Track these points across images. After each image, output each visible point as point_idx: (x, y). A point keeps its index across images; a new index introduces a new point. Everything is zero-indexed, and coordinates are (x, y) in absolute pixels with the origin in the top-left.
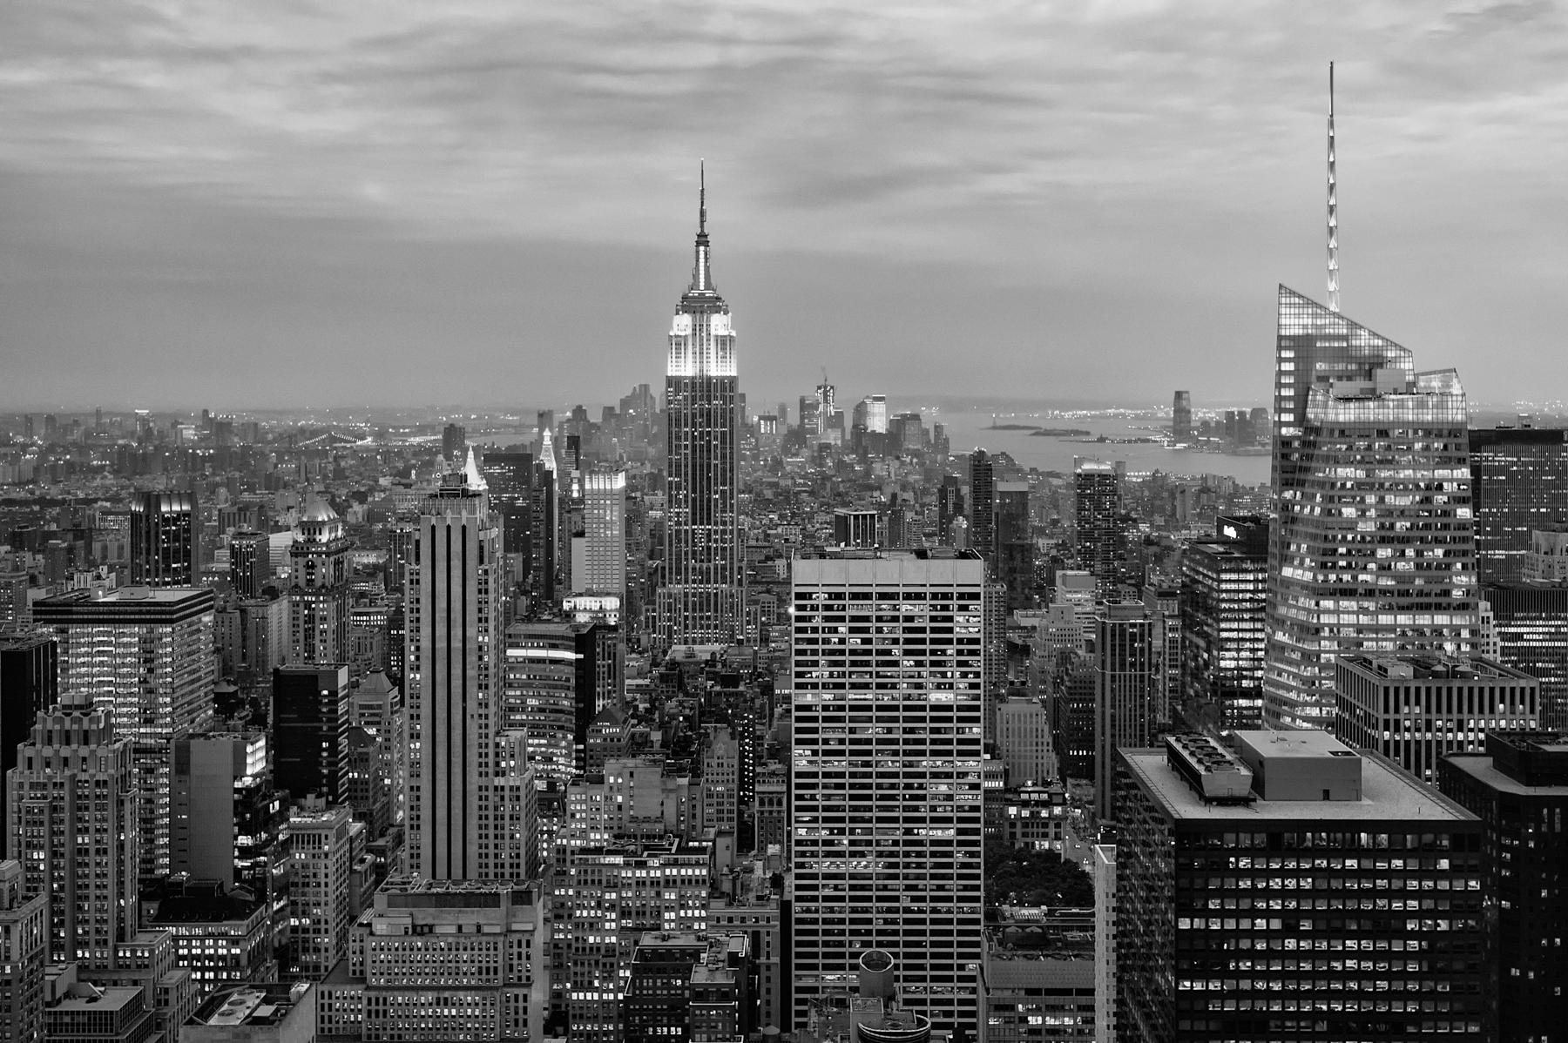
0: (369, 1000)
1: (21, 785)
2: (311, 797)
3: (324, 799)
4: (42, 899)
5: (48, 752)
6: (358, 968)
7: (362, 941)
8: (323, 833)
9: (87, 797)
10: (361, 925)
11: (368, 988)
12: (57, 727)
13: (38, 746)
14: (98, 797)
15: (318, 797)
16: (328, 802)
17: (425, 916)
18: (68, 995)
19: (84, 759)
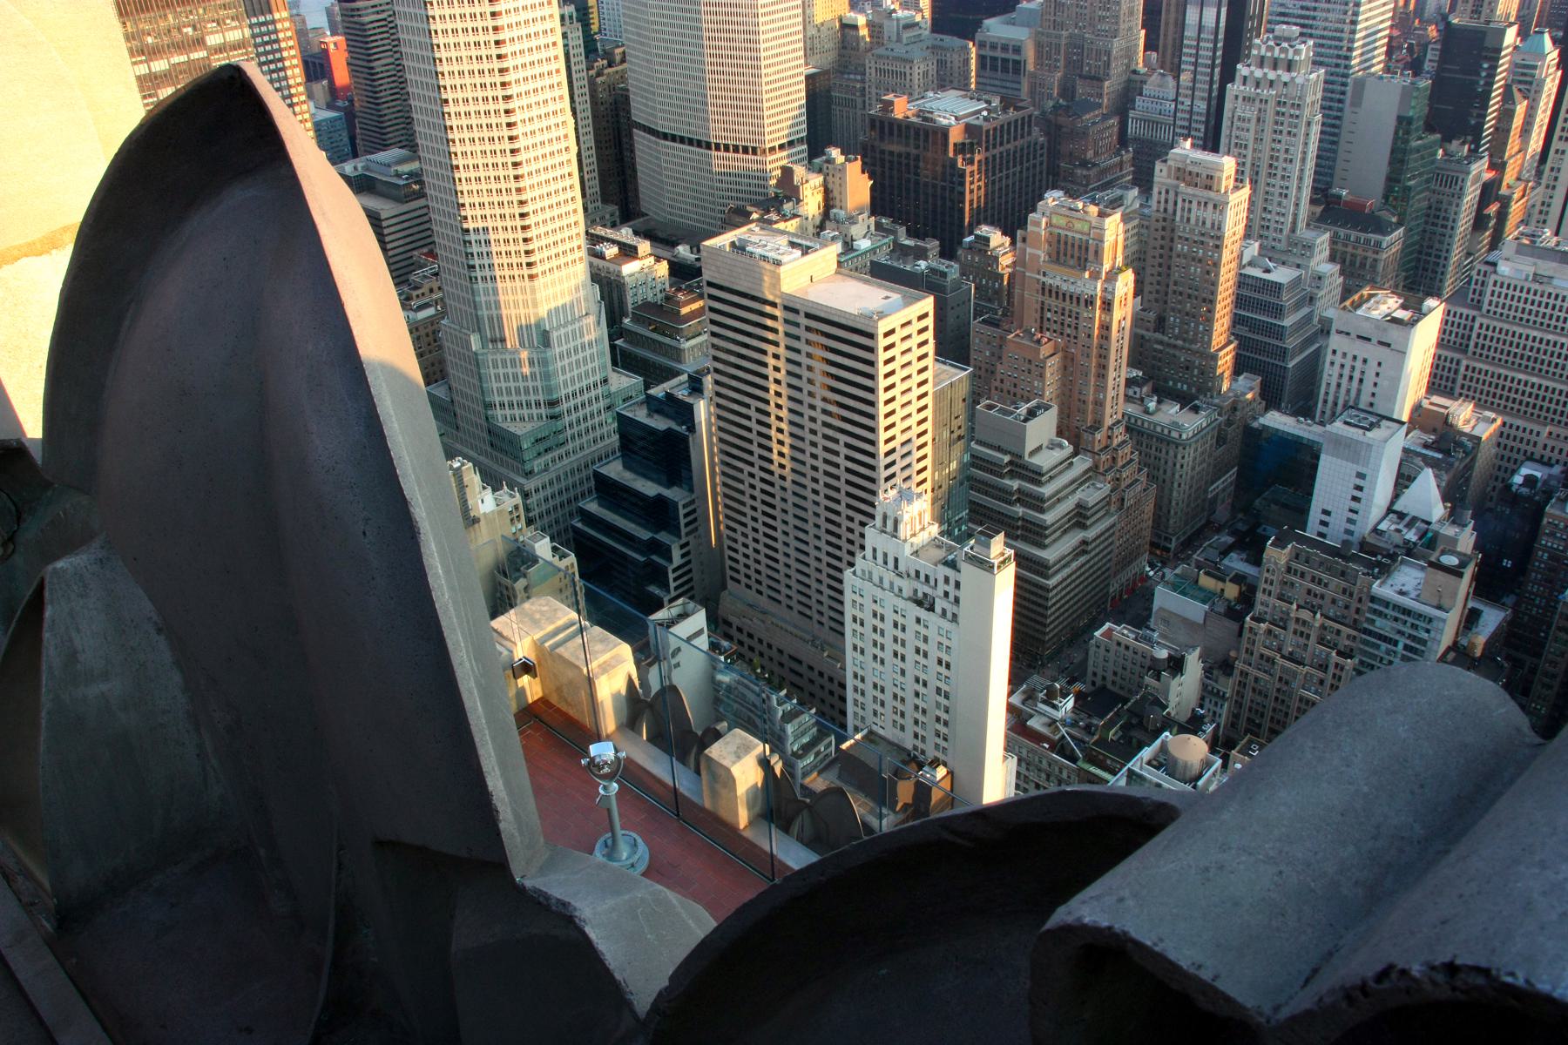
0: (1481, 325)
1: (1237, 97)
2: (1455, 143)
3: (1466, 147)
4: (1246, 192)
5: (1258, 73)
6: (1476, 297)
7: (1485, 275)
8: (1461, 176)
9: (1283, 114)
10: (1487, 263)
11: (1483, 316)
12: (1269, 54)
13: (1253, 68)
14: (1291, 116)
15: (1463, 143)
16: (1469, 150)
17: (1547, 267)
18: (1250, 264)
19: (1285, 84)
